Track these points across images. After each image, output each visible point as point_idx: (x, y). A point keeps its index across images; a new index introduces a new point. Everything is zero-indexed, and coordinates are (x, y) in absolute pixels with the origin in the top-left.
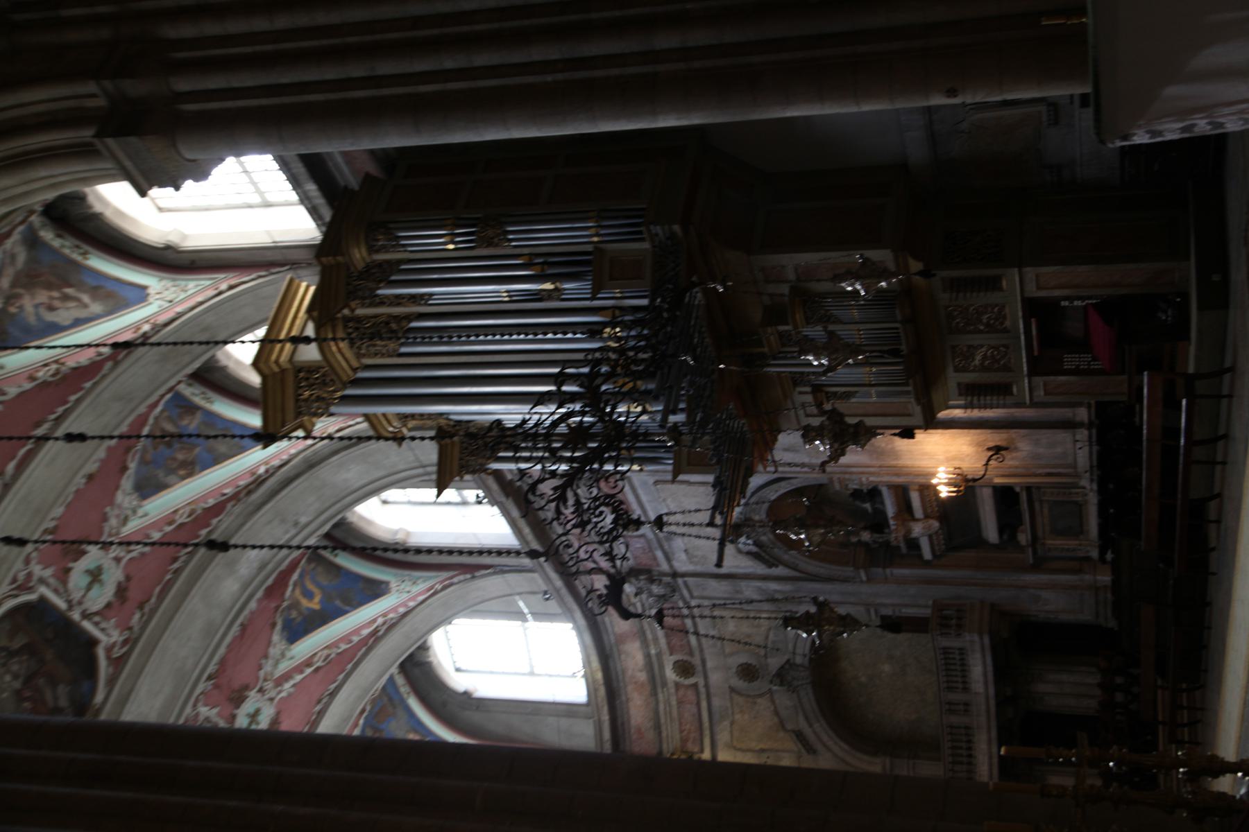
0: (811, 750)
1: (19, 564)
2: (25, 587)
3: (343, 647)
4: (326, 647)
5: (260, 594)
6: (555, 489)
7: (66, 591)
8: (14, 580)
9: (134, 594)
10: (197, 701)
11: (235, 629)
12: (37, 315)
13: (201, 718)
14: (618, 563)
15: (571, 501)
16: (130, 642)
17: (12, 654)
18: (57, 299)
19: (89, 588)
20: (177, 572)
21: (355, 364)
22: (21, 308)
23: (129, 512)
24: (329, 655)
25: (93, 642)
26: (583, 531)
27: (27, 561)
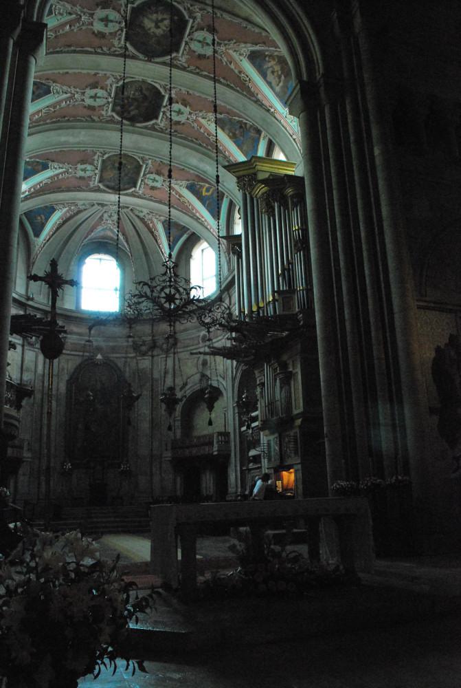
0: (181, 389)
6: (145, 293)
9: (179, 127)
10: (153, 159)
11: (183, 167)
12: (268, 68)
13: (147, 162)
15: (140, 300)
16: (162, 131)
18: (278, 74)
21: (258, 196)
22: (269, 62)
23: (208, 119)
25: (157, 118)
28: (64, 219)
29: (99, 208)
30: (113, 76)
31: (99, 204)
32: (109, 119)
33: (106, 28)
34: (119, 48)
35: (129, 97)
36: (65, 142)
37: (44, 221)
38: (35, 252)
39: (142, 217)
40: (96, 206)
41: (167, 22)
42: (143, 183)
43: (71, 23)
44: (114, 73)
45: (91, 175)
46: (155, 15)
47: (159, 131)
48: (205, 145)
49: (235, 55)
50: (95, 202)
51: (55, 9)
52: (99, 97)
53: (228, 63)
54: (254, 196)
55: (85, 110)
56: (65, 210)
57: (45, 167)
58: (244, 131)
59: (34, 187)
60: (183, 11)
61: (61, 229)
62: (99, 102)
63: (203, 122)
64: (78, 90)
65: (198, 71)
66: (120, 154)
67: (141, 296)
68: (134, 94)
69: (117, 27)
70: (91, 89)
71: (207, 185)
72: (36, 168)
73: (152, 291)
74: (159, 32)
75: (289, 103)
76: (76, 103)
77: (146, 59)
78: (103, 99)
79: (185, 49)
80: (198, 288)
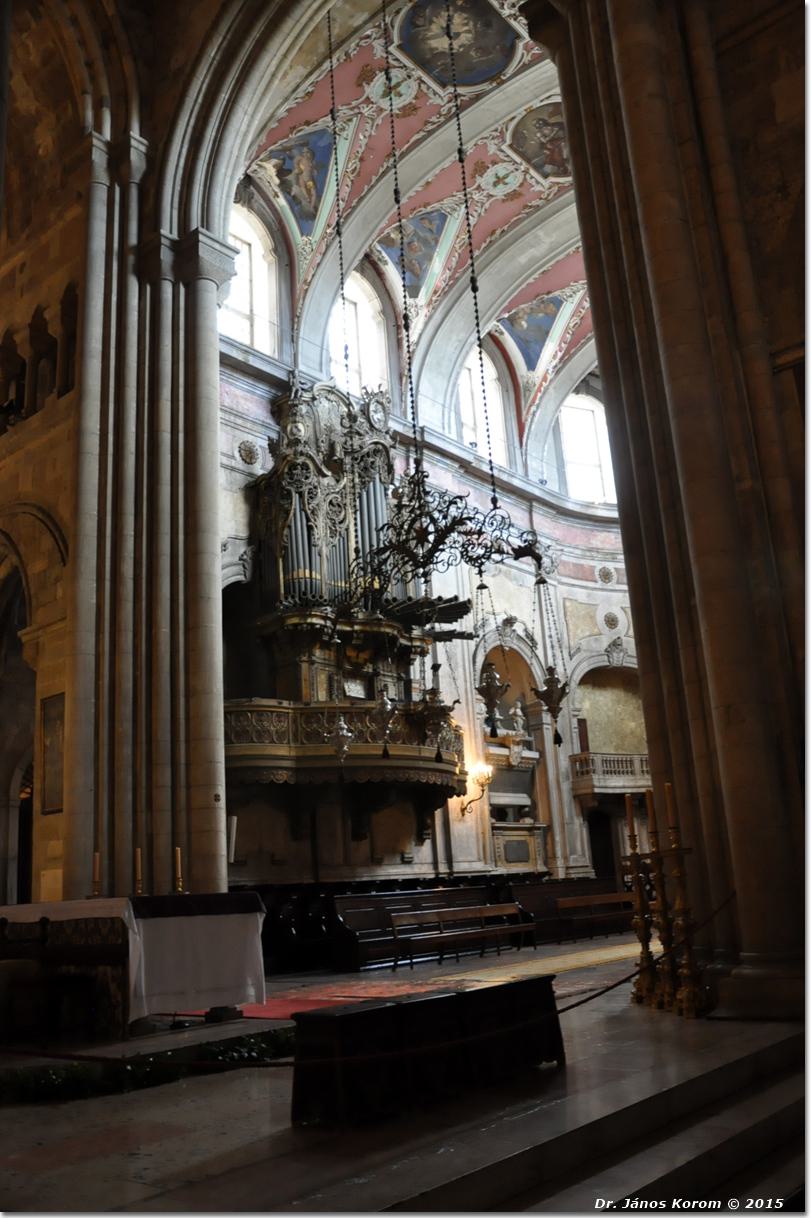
6: (390, 542)
17: (546, 124)
32: (556, 188)
33: (402, 98)
34: (449, 101)
35: (542, 143)
41: (458, 19)
44: (485, 134)
46: (434, 27)
52: (506, 176)
55: (507, 203)
59: (563, 340)
62: (514, 181)
68: (545, 136)
69: (414, 85)
70: (481, 176)
73: (399, 534)
74: (465, 38)
76: (487, 205)
77: (494, 84)
80: (458, 500)
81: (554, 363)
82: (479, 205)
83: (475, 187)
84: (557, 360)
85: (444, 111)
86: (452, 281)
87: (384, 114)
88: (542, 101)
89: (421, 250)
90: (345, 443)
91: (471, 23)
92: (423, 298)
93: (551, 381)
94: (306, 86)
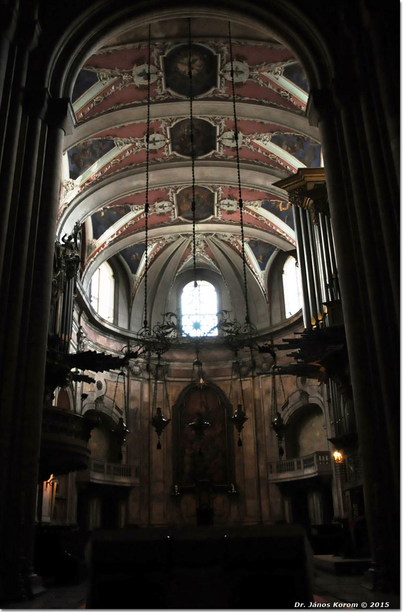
0: (283, 408)
1: (220, 116)
2: (215, 122)
3: (269, 224)
4: (266, 219)
5: (265, 191)
6: (173, 323)
7: (223, 133)
8: (215, 117)
11: (251, 188)
14: (143, 354)
15: (168, 331)
16: (222, 159)
19: (229, 139)
20: (253, 163)
21: (309, 208)
24: (263, 221)
25: (215, 149)
26: (156, 338)
27: (222, 118)
28: (155, 253)
29: (185, 238)
30: (164, 120)
31: (183, 235)
32: (172, 157)
34: (163, 95)
35: (184, 135)
36: (137, 185)
37: (138, 258)
38: (134, 287)
39: (227, 241)
40: (182, 237)
42: (219, 209)
43: (115, 84)
45: (169, 210)
47: (220, 160)
48: (266, 164)
49: (270, 76)
50: (180, 234)
51: (99, 76)
53: (266, 85)
54: (305, 208)
56: (154, 245)
57: (128, 210)
58: (302, 144)
59: (121, 229)
60: (211, 49)
61: (154, 263)
62: (159, 145)
63: (258, 142)
64: (136, 139)
65: (239, 98)
66: (193, 186)
67: (169, 327)
71: (282, 202)
72: (120, 212)
75: (308, 115)
76: (139, 150)
78: (161, 141)
79: (221, 82)
80: (224, 312)
81: (111, 240)
82: (136, 148)
83: (141, 139)
84: (113, 239)
85: (158, 97)
86: (100, 179)
87: (133, 83)
88: (200, 117)
89: (89, 156)
90: (65, 250)
91: (201, 68)
92: (79, 181)
93: (106, 248)
94: (111, 49)
